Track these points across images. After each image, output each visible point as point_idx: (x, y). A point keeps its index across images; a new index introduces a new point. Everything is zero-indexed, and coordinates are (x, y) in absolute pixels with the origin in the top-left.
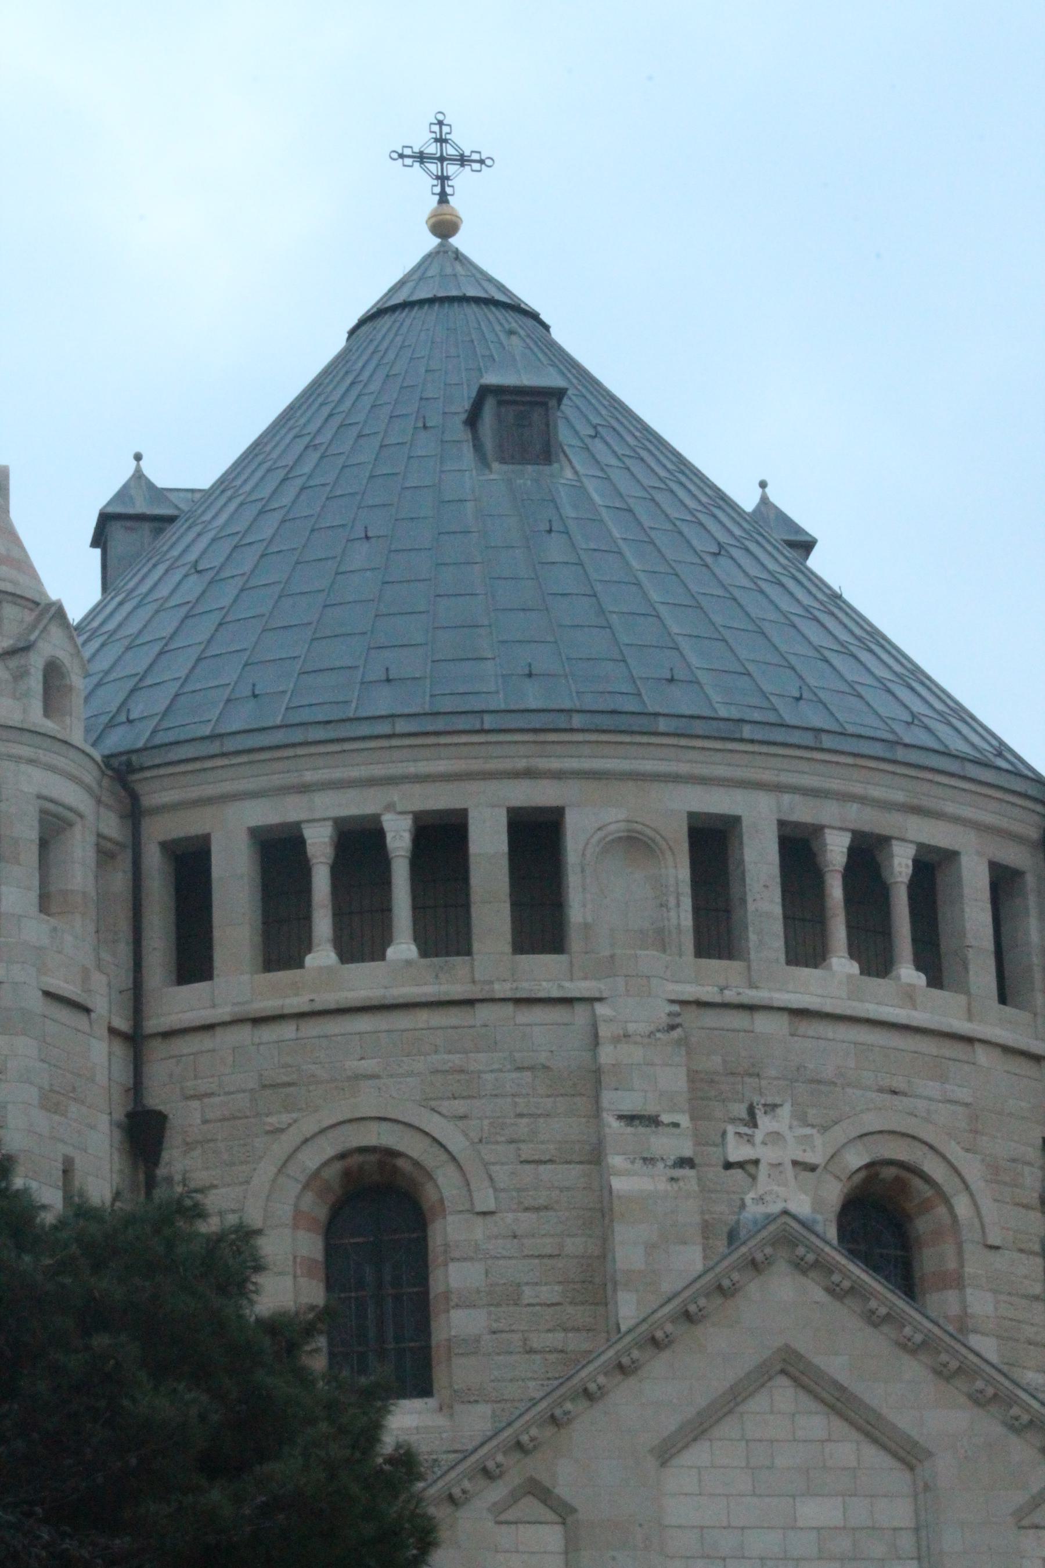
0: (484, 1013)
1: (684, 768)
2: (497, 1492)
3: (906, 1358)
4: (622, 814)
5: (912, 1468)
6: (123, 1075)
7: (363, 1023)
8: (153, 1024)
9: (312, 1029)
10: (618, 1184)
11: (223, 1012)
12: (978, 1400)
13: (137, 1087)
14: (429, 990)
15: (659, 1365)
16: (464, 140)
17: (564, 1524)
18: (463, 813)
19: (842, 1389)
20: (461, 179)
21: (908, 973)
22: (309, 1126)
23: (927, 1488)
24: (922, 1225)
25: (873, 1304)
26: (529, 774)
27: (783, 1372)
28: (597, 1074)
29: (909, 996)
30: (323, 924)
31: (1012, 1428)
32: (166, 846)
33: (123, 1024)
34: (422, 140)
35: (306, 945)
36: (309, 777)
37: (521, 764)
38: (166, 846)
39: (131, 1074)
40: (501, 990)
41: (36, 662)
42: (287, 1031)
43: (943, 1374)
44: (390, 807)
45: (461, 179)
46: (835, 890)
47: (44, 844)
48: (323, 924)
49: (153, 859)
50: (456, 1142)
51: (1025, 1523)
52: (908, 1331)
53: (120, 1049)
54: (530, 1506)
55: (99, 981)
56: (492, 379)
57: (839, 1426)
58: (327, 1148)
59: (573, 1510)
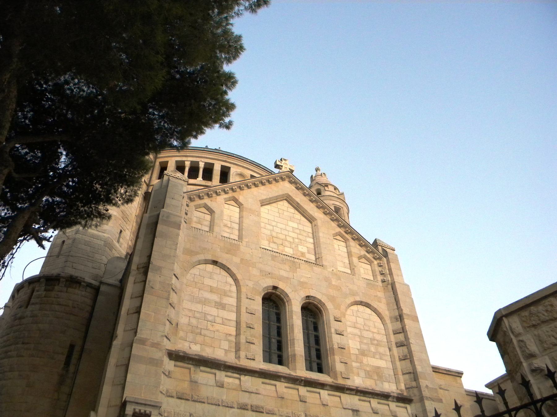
1: (251, 168)
2: (226, 196)
3: (311, 203)
4: (240, 171)
5: (311, 223)
12: (325, 213)
15: (262, 188)
17: (239, 208)
18: (214, 164)
19: (298, 204)
23: (315, 225)
25: (305, 191)
27: (286, 200)
31: (332, 220)
32: (160, 163)
36: (188, 154)
37: (224, 159)
38: (160, 163)
39: (146, 189)
43: (318, 207)
44: (201, 161)
51: (335, 238)
52: (312, 197)
54: (233, 203)
57: (296, 212)
59: (242, 205)
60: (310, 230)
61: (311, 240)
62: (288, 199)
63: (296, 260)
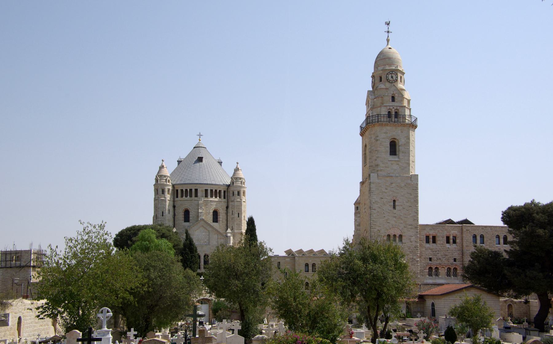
0: (193, 201)
6: (173, 203)
7: (186, 201)
8: (175, 200)
9: (183, 201)
10: (199, 211)
11: (178, 200)
13: (174, 204)
14: (190, 199)
16: (201, 134)
20: (201, 137)
21: (218, 198)
22: (183, 207)
24: (218, 212)
26: (196, 187)
28: (198, 205)
29: (218, 199)
30: (184, 195)
33: (173, 200)
34: (198, 134)
35: (183, 196)
40: (194, 199)
41: (167, 180)
42: (182, 201)
45: (201, 137)
46: (214, 193)
47: (168, 191)
48: (184, 195)
49: (175, 190)
50: (191, 208)
53: (173, 202)
55: (171, 198)
56: (199, 156)
58: (184, 208)
60: (208, 234)
61: (208, 237)
62: (203, 226)
63: (203, 245)
